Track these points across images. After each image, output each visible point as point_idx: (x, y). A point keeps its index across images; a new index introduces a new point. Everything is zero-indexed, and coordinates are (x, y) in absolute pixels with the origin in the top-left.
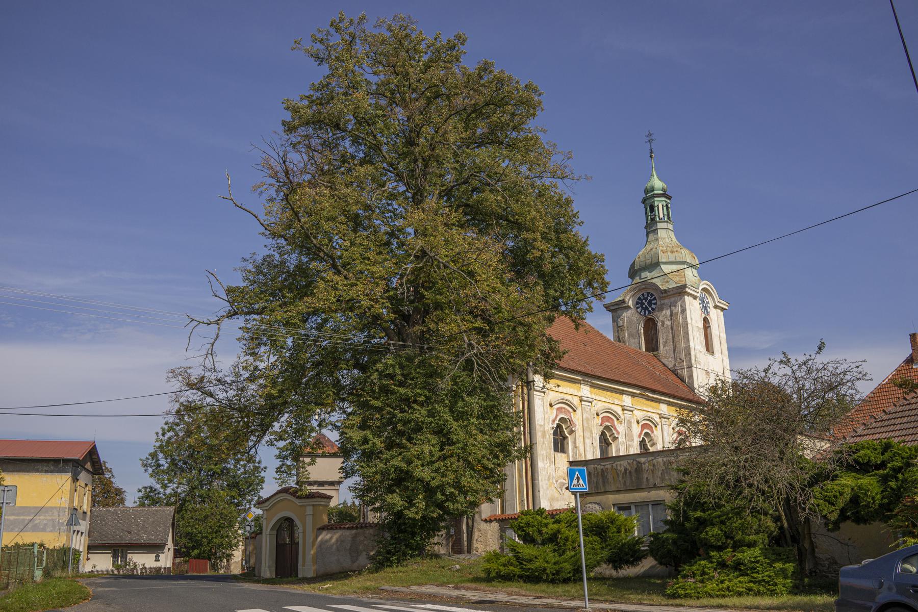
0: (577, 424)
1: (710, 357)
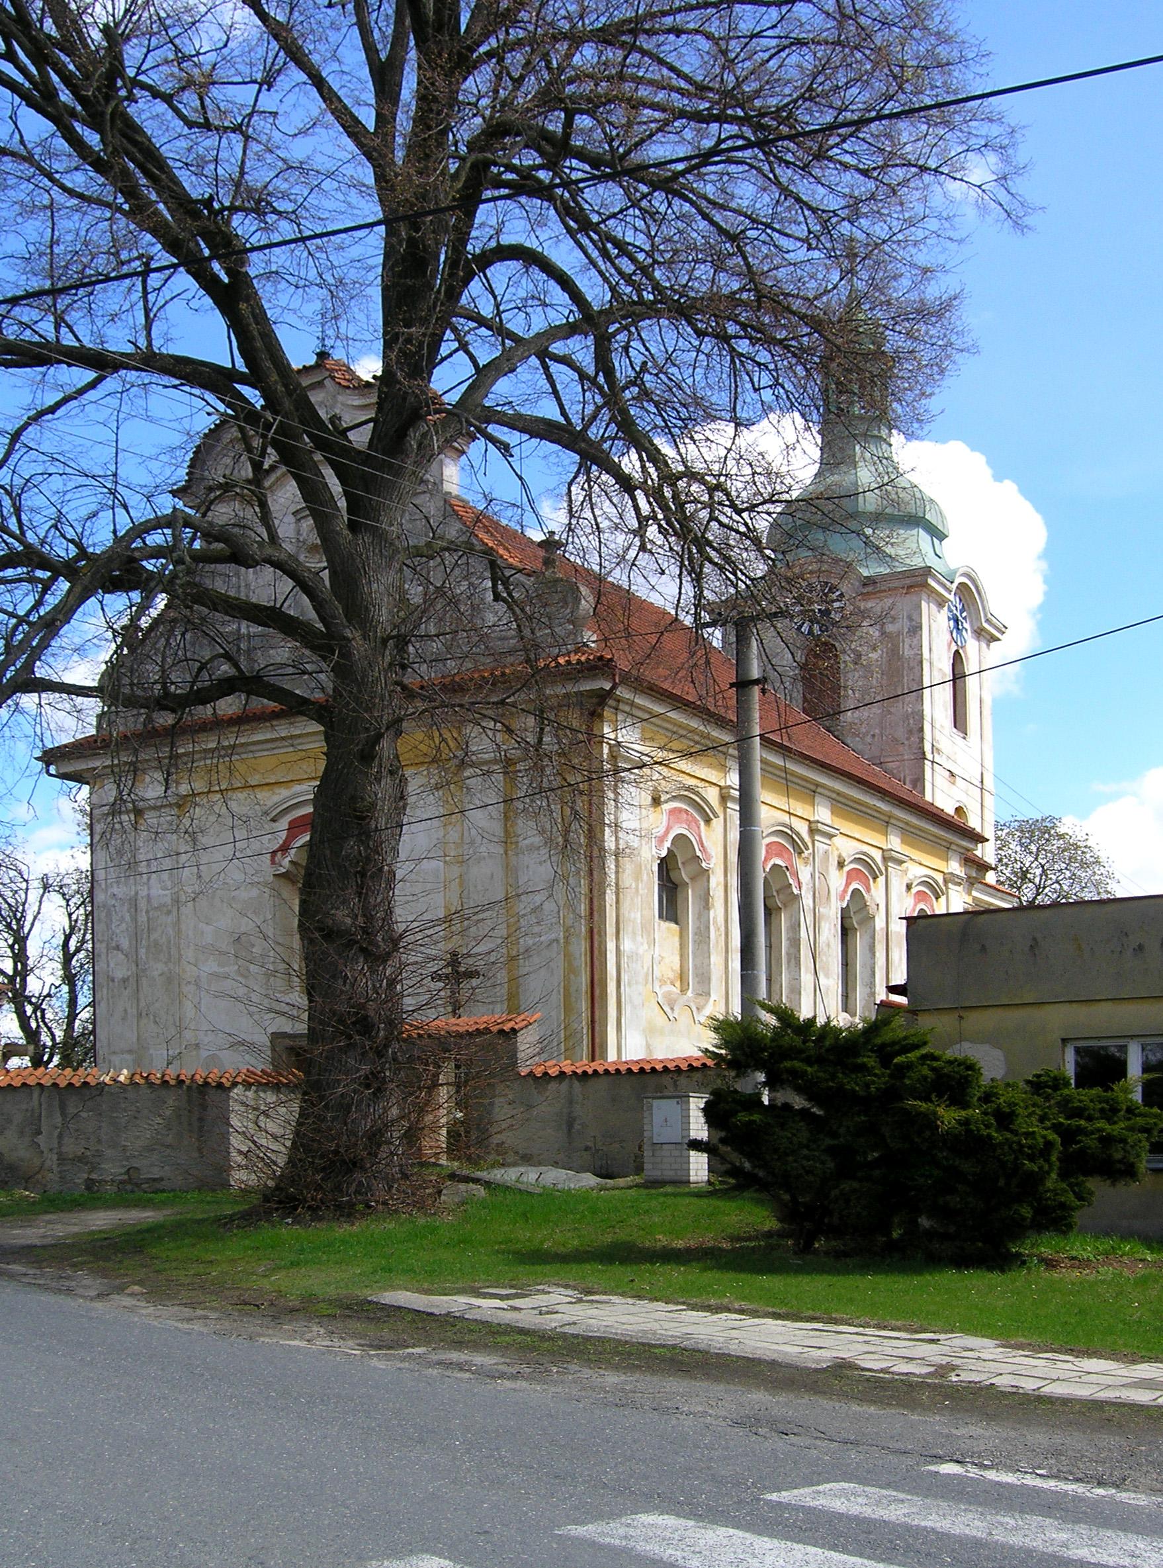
0: (713, 854)
1: (957, 736)
